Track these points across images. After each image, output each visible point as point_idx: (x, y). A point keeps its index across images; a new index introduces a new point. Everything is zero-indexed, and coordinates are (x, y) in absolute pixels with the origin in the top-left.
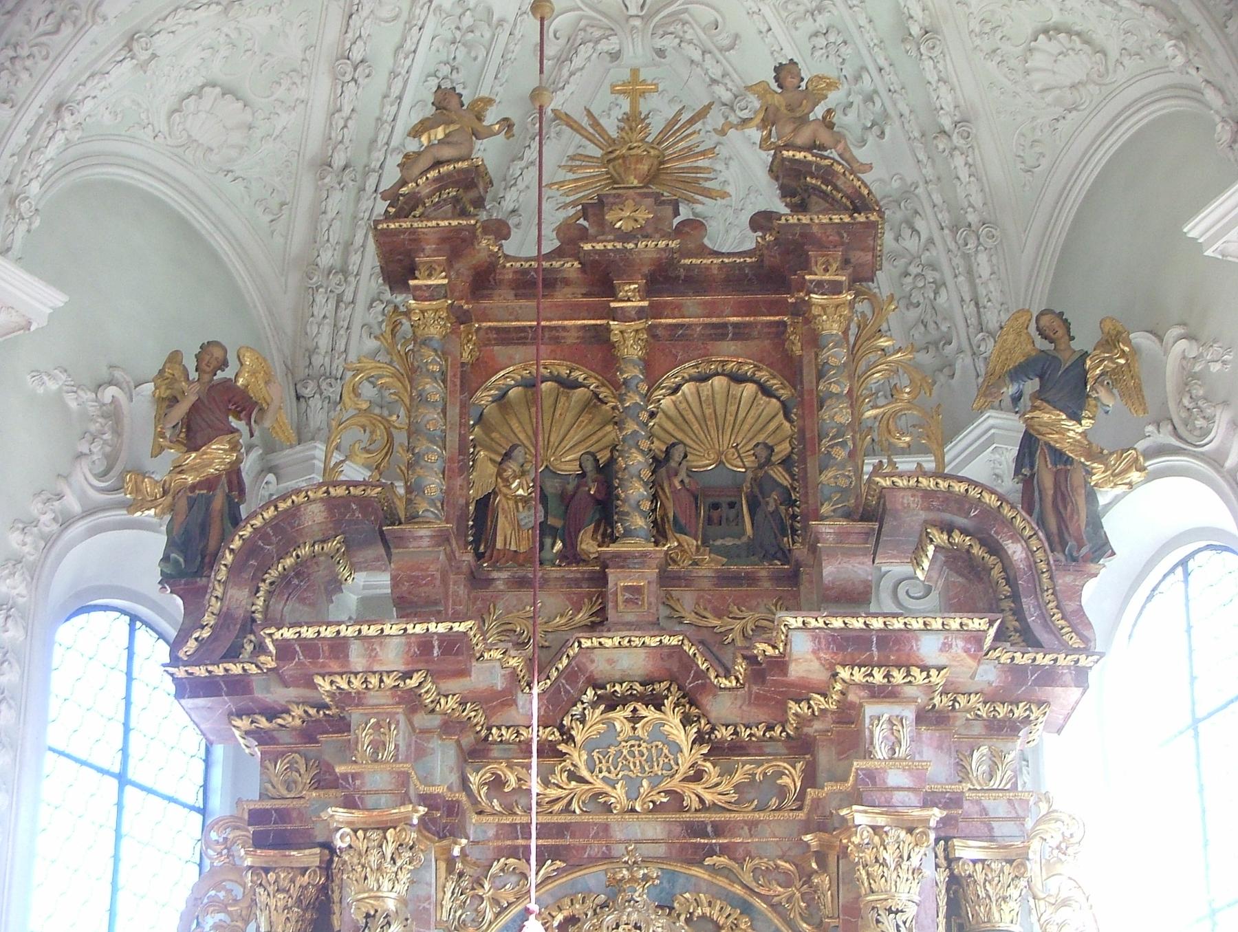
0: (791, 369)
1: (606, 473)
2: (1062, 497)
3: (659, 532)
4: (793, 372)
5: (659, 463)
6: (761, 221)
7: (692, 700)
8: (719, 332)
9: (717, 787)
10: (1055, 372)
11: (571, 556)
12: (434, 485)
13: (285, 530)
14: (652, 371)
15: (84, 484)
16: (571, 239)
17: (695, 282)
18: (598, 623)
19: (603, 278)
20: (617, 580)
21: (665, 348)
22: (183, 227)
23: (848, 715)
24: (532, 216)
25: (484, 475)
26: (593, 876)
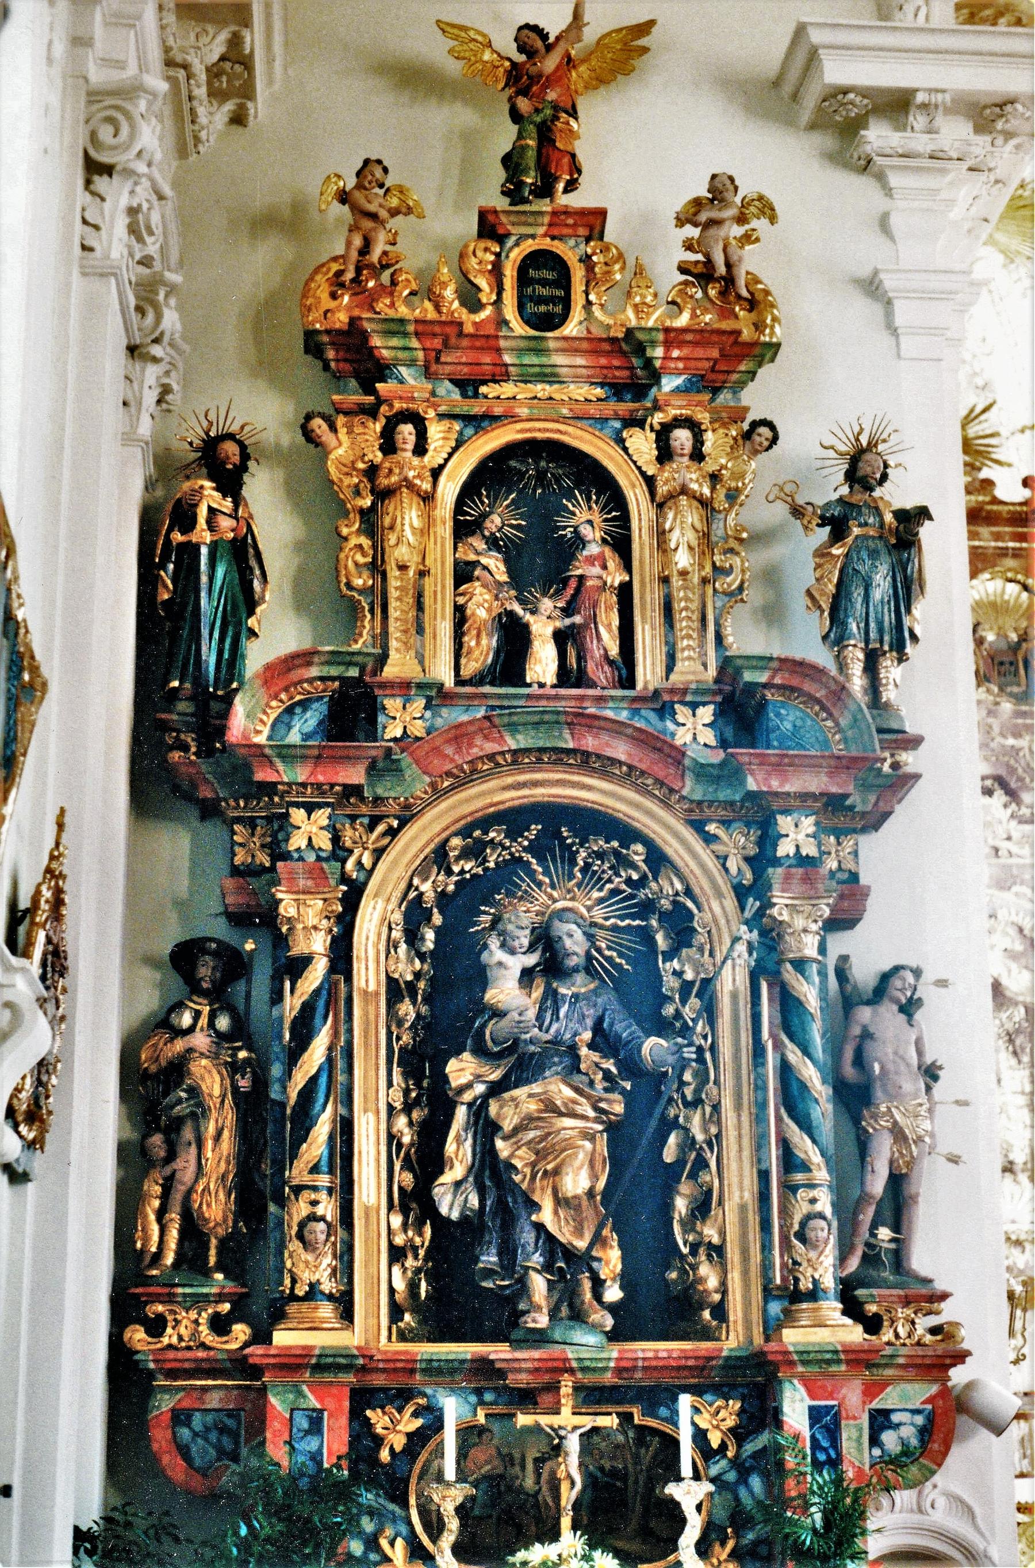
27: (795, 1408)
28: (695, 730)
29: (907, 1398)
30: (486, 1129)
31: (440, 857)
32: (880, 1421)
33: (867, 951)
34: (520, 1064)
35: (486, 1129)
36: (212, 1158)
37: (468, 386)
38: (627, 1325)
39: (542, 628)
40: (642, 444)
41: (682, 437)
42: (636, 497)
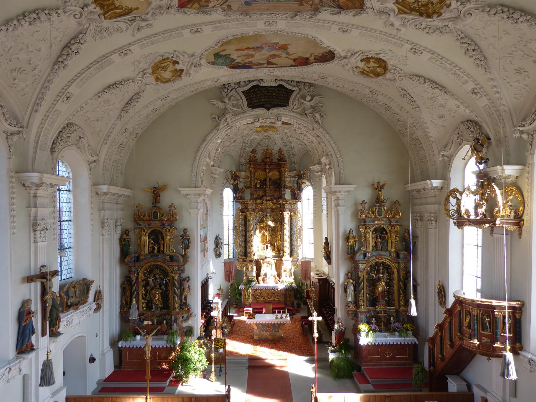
0: (280, 173)
1: (265, 180)
2: (300, 187)
3: (269, 186)
4: (280, 173)
5: (270, 179)
6: (278, 159)
7: (272, 201)
8: (274, 169)
9: (274, 207)
10: (300, 176)
11: (263, 187)
12: (253, 184)
13: (242, 189)
14: (269, 173)
15: (225, 181)
16: (263, 161)
17: (273, 165)
18: (265, 195)
19: (265, 165)
20: (267, 192)
21: (271, 170)
22: (230, 155)
23: (284, 204)
24: (259, 156)
25: (256, 181)
26: (265, 213)
27: (173, 318)
28: (168, 258)
29: (185, 315)
30: (150, 293)
31: (146, 269)
32: (183, 317)
33: (184, 276)
34: (152, 289)
35: (150, 293)
36: (128, 294)
37: (149, 225)
38: (162, 308)
39: (156, 248)
40: (164, 231)
41: (167, 230)
42: (164, 235)
